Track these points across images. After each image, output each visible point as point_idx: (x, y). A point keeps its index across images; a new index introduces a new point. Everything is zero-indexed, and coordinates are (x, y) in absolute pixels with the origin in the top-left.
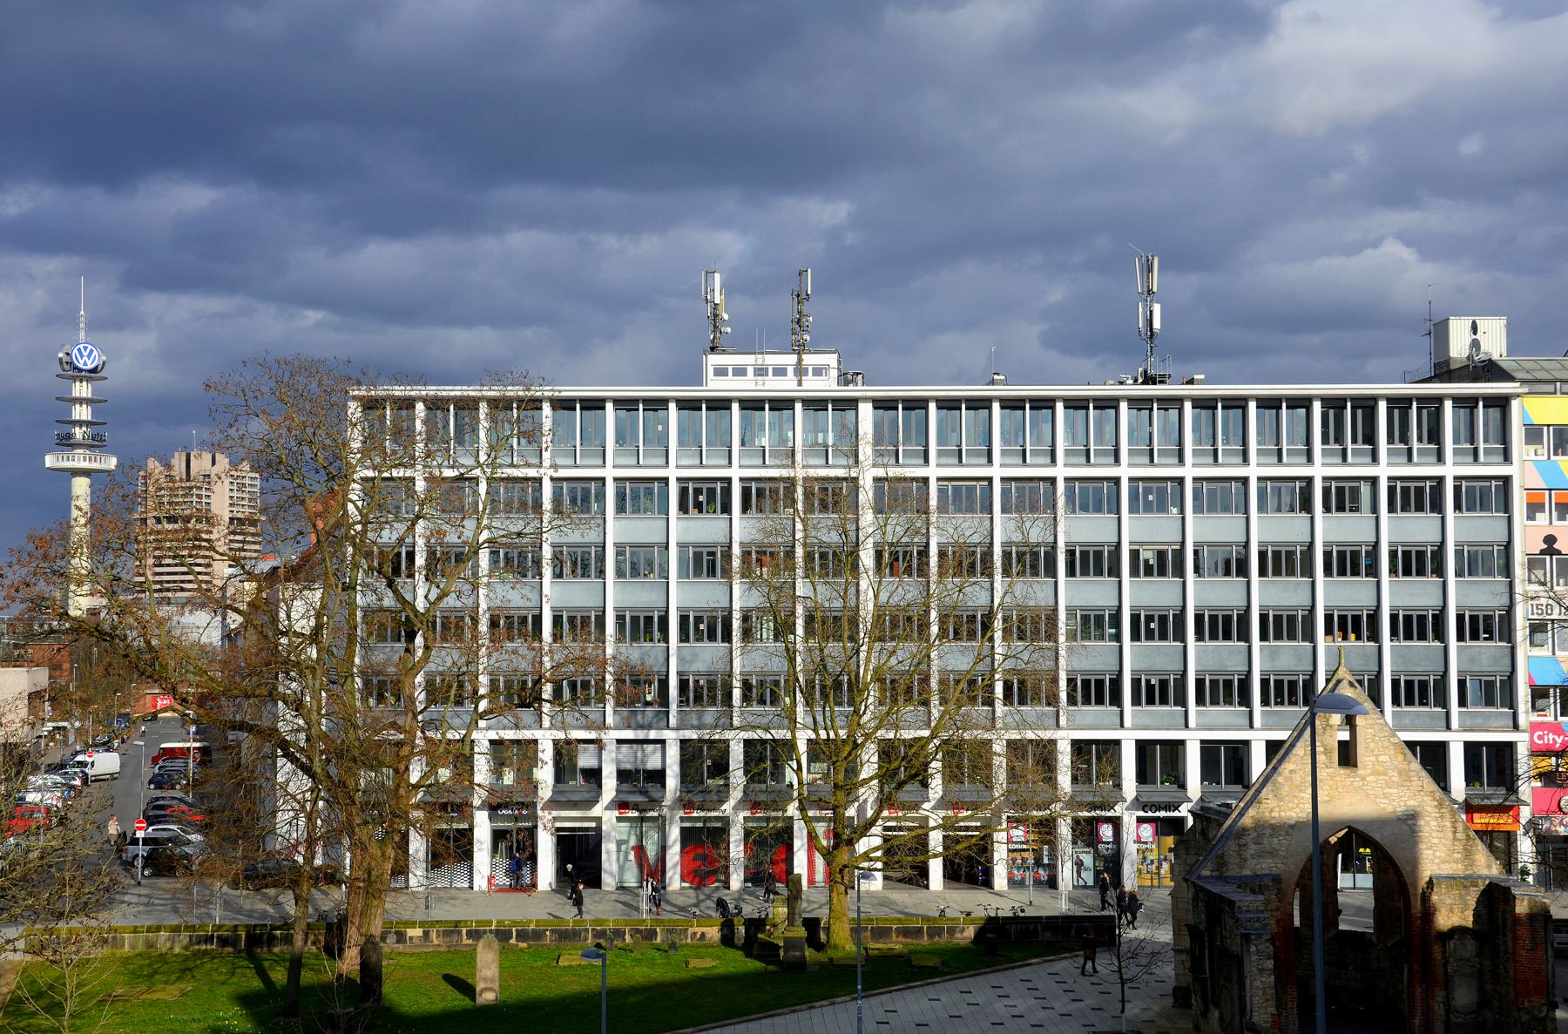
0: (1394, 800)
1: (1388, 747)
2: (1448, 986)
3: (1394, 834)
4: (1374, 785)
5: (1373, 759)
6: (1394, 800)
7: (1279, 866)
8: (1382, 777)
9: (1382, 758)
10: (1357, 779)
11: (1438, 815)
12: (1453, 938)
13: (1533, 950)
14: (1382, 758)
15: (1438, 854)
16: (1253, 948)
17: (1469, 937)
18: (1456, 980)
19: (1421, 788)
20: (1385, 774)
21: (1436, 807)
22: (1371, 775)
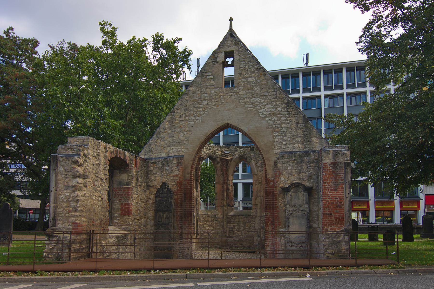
0: (257, 105)
1: (254, 72)
2: (287, 225)
3: (256, 127)
4: (245, 96)
5: (243, 80)
6: (257, 105)
8: (250, 91)
9: (249, 79)
10: (234, 94)
11: (286, 113)
12: (290, 191)
13: (335, 190)
14: (249, 79)
15: (285, 138)
16: (61, 169)
17: (301, 190)
18: (291, 220)
19: (275, 97)
20: (251, 89)
21: (285, 107)
22: (242, 90)
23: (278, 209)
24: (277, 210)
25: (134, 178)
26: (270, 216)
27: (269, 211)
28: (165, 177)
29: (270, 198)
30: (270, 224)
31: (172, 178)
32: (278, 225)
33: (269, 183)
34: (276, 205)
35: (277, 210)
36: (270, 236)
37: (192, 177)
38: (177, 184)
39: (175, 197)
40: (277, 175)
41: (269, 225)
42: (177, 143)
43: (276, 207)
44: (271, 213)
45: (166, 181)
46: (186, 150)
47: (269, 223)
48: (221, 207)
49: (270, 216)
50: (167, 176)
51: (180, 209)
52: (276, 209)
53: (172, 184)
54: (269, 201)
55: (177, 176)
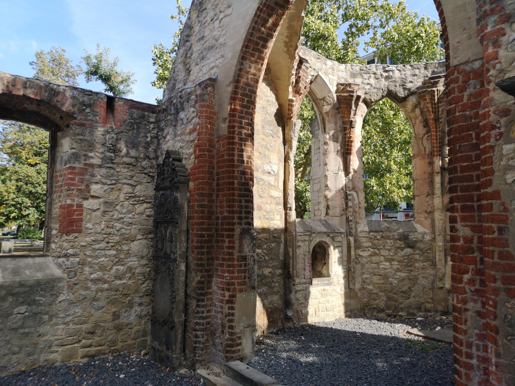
7: (218, 63)
23: (495, 211)
24: (495, 211)
25: (98, 146)
26: (468, 240)
27: (463, 219)
28: (179, 138)
29: (468, 158)
30: (471, 282)
31: (187, 138)
32: (503, 295)
33: (463, 89)
34: (490, 183)
35: (495, 211)
36: (474, 340)
37: (234, 127)
38: (195, 151)
39: (192, 184)
40: (489, 29)
41: (467, 287)
42: (209, 50)
43: (485, 197)
44: (474, 229)
45: (181, 147)
46: (221, 60)
47: (466, 277)
48: (427, 213)
49: (471, 240)
50: (181, 135)
51: (199, 218)
52: (490, 207)
53: (188, 151)
54: (463, 169)
55: (194, 130)
